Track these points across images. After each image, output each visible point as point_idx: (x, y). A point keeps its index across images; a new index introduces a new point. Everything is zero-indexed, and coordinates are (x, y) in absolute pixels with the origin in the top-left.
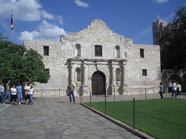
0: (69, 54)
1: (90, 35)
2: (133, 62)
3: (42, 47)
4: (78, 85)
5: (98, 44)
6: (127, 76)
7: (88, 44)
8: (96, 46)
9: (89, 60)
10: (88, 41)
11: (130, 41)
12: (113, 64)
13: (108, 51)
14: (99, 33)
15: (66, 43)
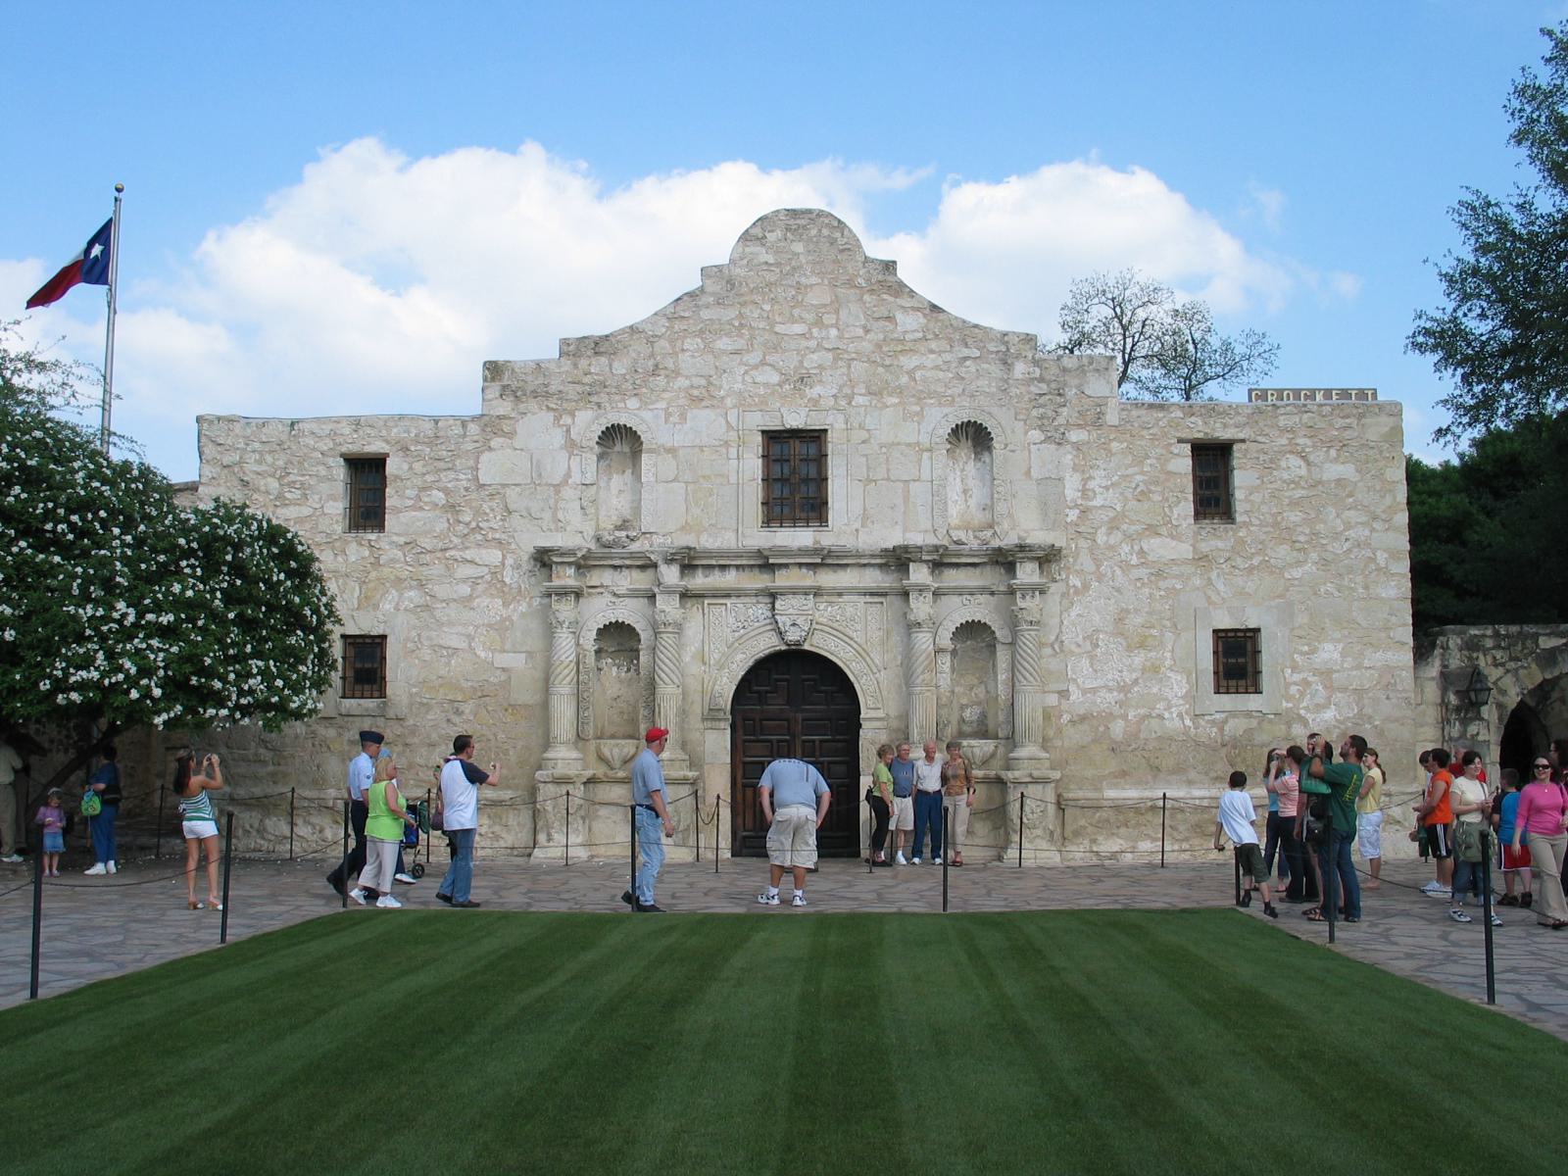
0: (547, 515)
1: (723, 343)
2: (1126, 566)
3: (331, 461)
4: (612, 769)
5: (795, 420)
6: (1064, 694)
7: (706, 423)
8: (776, 440)
9: (709, 554)
10: (703, 396)
11: (1091, 377)
12: (921, 589)
13: (881, 473)
14: (798, 328)
15: (522, 427)
